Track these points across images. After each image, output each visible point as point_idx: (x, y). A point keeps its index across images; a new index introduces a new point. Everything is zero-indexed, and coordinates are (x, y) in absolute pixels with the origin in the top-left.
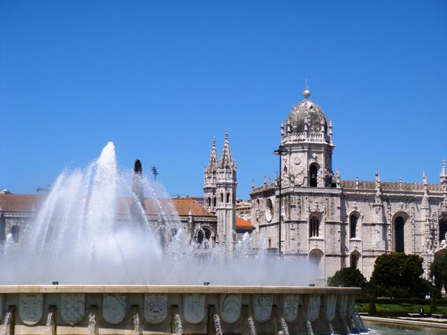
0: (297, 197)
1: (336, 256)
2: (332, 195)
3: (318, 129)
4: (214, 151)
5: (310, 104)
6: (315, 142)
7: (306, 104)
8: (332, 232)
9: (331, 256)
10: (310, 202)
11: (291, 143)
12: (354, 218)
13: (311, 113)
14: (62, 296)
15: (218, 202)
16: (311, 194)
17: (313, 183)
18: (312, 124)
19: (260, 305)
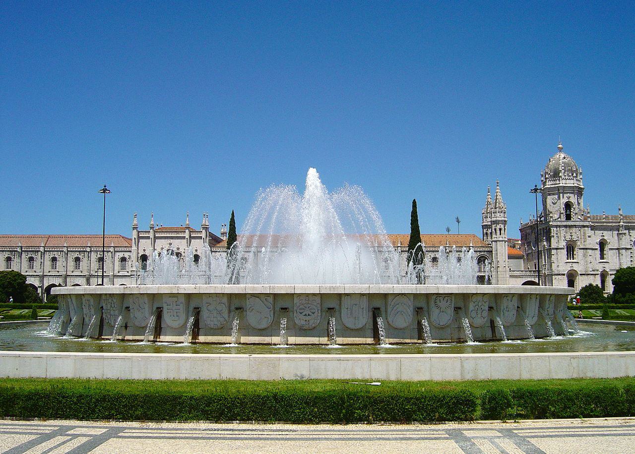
0: (555, 229)
1: (588, 274)
2: (584, 226)
3: (570, 174)
4: (489, 196)
5: (562, 155)
6: (568, 185)
7: (560, 156)
8: (585, 256)
9: (584, 274)
10: (566, 233)
11: (549, 186)
12: (602, 244)
13: (563, 163)
14: (204, 297)
15: (494, 236)
16: (566, 226)
17: (568, 217)
18: (565, 171)
19: (438, 307)
